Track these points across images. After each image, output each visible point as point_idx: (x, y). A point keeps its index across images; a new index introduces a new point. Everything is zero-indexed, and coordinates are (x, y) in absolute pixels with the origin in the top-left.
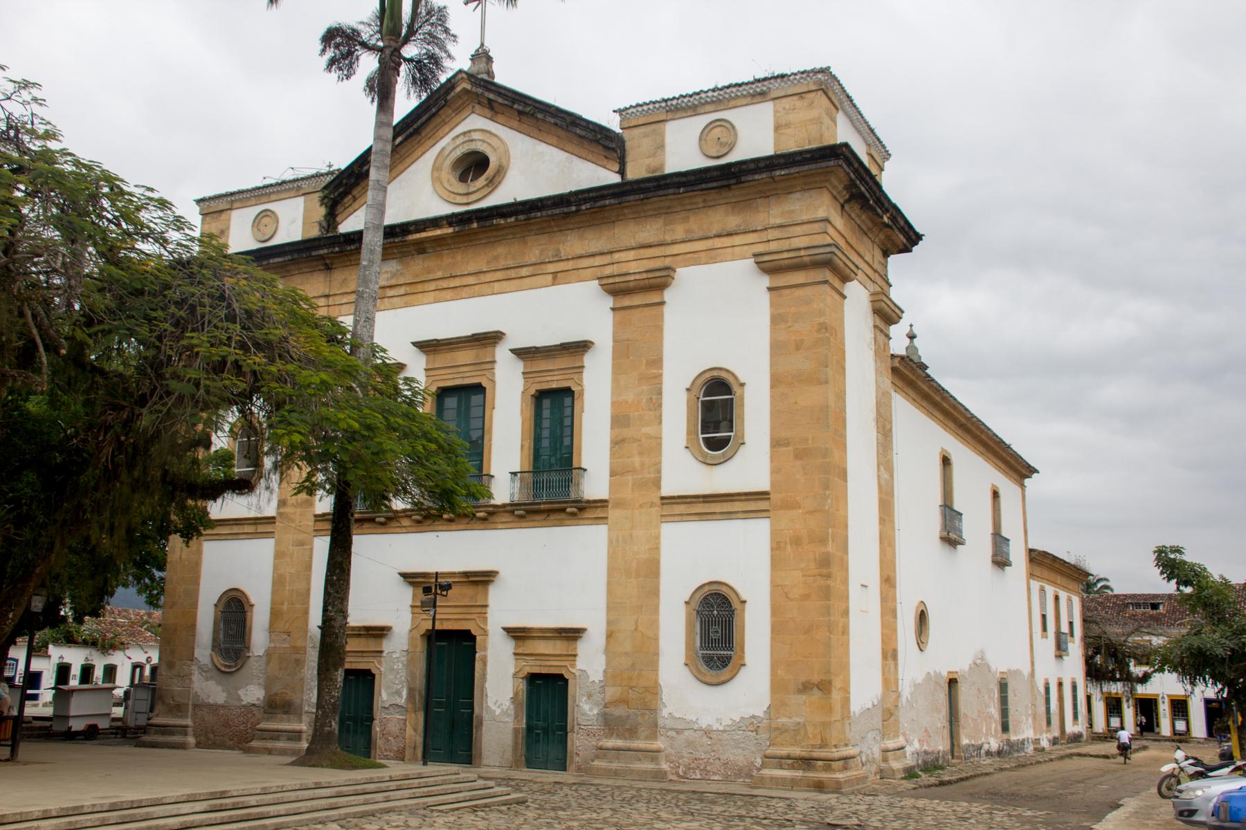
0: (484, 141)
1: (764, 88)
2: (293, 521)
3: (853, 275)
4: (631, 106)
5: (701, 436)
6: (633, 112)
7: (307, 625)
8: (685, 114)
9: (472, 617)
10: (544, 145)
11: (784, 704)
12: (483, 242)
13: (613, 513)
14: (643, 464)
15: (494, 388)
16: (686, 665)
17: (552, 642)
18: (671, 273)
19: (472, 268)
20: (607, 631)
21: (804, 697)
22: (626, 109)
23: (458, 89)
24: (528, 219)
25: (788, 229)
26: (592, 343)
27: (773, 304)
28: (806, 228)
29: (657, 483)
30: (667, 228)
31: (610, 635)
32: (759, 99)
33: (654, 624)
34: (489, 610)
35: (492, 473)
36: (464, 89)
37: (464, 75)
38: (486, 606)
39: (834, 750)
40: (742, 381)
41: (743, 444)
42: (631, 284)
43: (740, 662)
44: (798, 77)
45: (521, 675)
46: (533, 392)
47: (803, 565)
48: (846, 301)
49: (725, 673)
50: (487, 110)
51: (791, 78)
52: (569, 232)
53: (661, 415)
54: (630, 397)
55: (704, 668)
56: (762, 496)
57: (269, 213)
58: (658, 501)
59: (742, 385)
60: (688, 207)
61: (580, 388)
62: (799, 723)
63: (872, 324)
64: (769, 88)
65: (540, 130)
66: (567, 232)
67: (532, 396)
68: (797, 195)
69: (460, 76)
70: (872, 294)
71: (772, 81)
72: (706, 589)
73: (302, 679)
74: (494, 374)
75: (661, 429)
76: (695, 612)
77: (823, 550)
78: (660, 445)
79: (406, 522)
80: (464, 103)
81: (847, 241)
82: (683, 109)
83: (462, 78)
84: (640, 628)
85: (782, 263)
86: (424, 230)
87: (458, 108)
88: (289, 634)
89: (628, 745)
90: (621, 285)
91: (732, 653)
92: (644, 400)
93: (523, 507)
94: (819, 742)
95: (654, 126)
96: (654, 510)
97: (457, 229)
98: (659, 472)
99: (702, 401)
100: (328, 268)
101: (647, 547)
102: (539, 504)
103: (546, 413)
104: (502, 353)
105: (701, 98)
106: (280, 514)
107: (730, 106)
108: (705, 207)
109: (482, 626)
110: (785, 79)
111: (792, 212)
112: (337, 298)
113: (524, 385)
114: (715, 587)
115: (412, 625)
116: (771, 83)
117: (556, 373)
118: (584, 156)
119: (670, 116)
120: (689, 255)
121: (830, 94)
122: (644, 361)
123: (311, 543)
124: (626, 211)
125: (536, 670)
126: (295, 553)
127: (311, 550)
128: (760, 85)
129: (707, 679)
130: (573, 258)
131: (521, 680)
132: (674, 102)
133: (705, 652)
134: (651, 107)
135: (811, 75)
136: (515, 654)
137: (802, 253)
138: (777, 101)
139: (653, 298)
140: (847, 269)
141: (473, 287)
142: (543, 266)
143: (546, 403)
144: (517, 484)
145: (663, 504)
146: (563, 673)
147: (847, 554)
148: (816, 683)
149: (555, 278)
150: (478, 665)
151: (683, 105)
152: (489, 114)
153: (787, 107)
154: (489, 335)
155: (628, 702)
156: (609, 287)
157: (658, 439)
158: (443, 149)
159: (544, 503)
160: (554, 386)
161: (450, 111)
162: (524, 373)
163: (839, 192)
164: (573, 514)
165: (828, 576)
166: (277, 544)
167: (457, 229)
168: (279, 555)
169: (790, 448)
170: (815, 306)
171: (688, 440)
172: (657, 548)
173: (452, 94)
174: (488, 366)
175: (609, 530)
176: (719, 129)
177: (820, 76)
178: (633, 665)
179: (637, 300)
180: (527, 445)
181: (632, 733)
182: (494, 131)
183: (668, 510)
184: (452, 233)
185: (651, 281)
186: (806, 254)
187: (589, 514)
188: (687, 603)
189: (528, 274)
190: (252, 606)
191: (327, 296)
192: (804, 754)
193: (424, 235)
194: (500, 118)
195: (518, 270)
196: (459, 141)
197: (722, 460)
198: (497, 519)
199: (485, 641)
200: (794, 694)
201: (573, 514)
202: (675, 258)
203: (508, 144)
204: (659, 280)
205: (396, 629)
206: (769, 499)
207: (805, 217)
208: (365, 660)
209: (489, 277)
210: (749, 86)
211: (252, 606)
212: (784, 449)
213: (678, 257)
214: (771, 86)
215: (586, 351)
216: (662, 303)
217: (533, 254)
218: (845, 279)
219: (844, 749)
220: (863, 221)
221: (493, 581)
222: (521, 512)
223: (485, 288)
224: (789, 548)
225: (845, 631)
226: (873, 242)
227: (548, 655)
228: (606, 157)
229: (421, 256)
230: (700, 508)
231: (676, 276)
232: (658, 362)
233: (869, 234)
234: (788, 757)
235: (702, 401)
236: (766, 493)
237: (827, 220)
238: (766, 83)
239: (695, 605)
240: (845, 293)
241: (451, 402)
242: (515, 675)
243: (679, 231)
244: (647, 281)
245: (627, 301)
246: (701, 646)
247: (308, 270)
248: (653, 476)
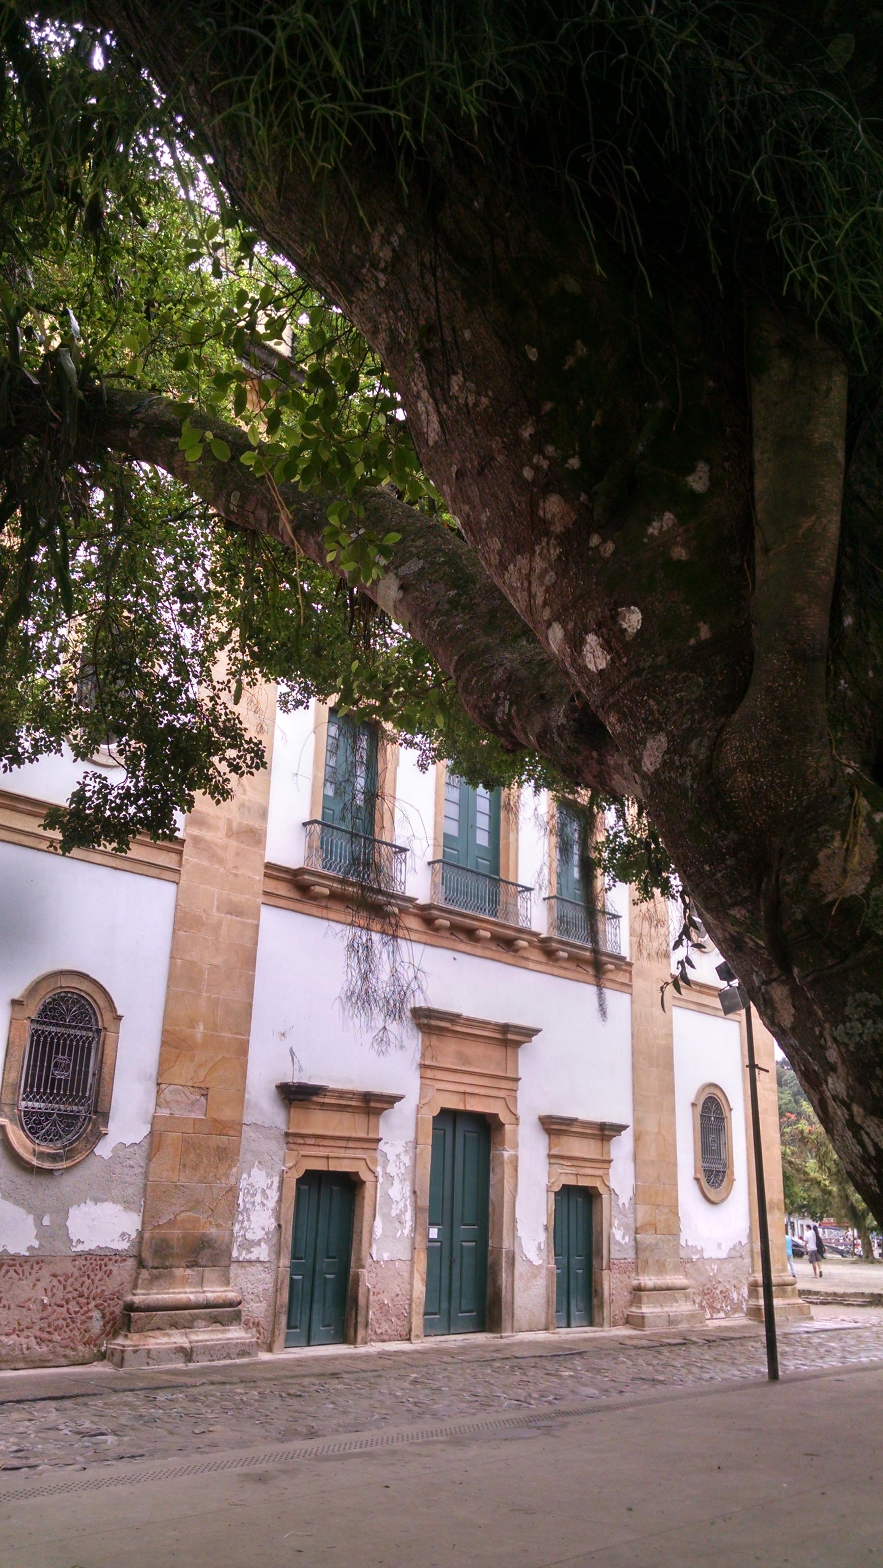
2: (221, 861)
7: (245, 1077)
38: (517, 1080)
73: (233, 1192)
88: (205, 1093)
93: (569, 949)
115: (421, 1097)
125: (572, 1181)
126: (224, 928)
127: (257, 926)
136: (550, 1156)
178: (659, 1177)
190: (119, 1018)
199: (515, 1133)
208: (350, 1153)
211: (119, 1018)
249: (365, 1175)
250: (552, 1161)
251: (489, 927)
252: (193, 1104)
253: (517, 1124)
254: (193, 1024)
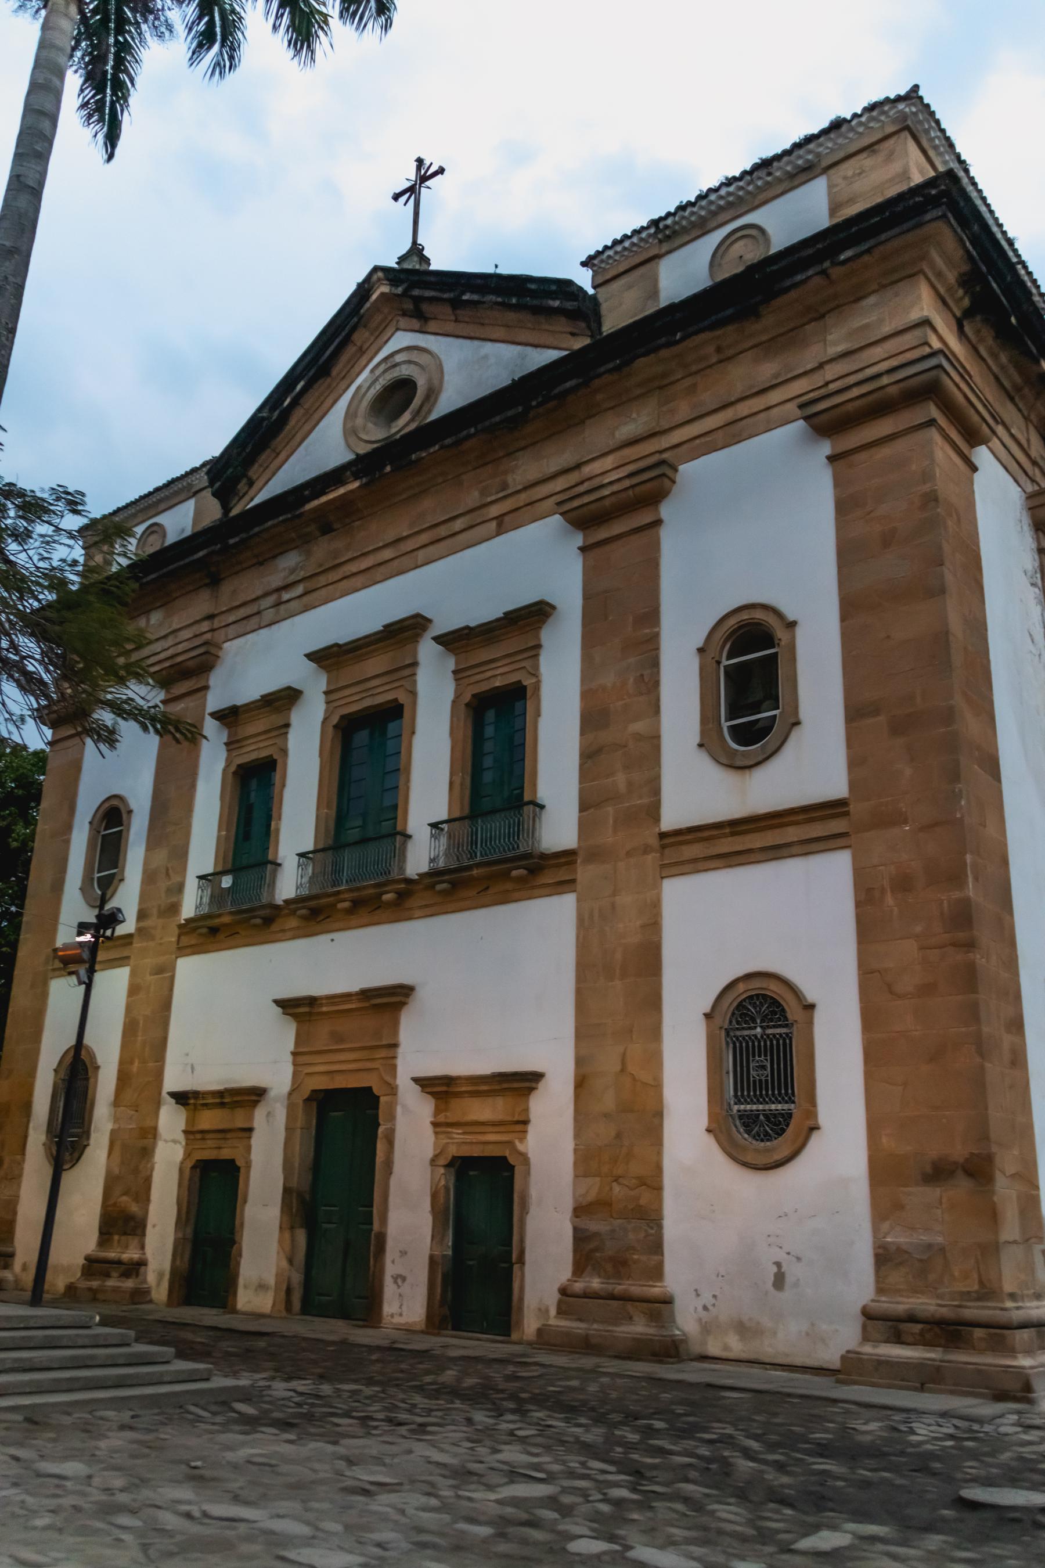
0: (409, 362)
1: (810, 157)
4: (606, 248)
5: (725, 725)
6: (609, 257)
8: (687, 238)
9: (375, 1065)
10: (489, 344)
11: (899, 1206)
12: (404, 496)
13: (584, 873)
14: (630, 784)
15: (414, 703)
16: (709, 1131)
17: (490, 1100)
18: (669, 472)
19: (390, 536)
20: (576, 1075)
21: (938, 1190)
22: (599, 253)
23: (374, 297)
24: (457, 443)
25: (857, 356)
26: (553, 607)
27: (838, 482)
28: (891, 346)
29: (654, 811)
30: (664, 409)
31: (581, 1083)
32: (803, 177)
33: (655, 1060)
34: (401, 1050)
35: (410, 831)
36: (382, 294)
37: (380, 274)
38: (395, 1046)
39: (1009, 1304)
40: (791, 617)
41: (798, 723)
42: (607, 503)
43: (810, 1123)
44: (863, 119)
45: (442, 1161)
46: (467, 697)
47: (918, 929)
48: (976, 476)
49: (781, 1146)
50: (415, 321)
51: (854, 123)
52: (520, 453)
53: (658, 700)
54: (608, 679)
55: (742, 1138)
56: (833, 808)
57: (155, 528)
58: (654, 842)
59: (792, 625)
60: (694, 368)
61: (534, 680)
62: (929, 1246)
63: (1034, 546)
64: (818, 155)
65: (483, 324)
66: (517, 454)
67: (467, 705)
68: (872, 300)
69: (375, 277)
70: (1030, 497)
71: (822, 139)
72: (741, 987)
74: (415, 682)
75: (659, 722)
76: (723, 1033)
77: (956, 895)
78: (657, 749)
79: (293, 923)
80: (386, 318)
82: (685, 230)
83: (379, 280)
84: (631, 1068)
85: (850, 407)
86: (323, 493)
87: (377, 327)
89: (610, 1287)
90: (593, 506)
91: (793, 1105)
92: (631, 680)
93: (446, 877)
94: (976, 1287)
95: (642, 270)
96: (649, 857)
97: (364, 480)
98: (656, 792)
99: (725, 667)
100: (214, 581)
101: (638, 923)
102: (469, 868)
103: (489, 731)
104: (427, 650)
105: (711, 203)
106: (139, 930)
107: (757, 203)
108: (720, 361)
109: (388, 1079)
110: (844, 128)
111: (866, 327)
112: (222, 617)
113: (456, 691)
114: (756, 984)
116: (821, 145)
117: (499, 664)
118: (542, 342)
119: (665, 247)
120: (698, 441)
121: (925, 144)
122: (631, 619)
123: (173, 969)
124: (599, 397)
125: (466, 1151)
127: (172, 979)
128: (801, 152)
129: (749, 1158)
130: (525, 489)
131: (442, 1170)
132: (669, 221)
133: (742, 1107)
134: (635, 240)
135: (886, 108)
136: (435, 1124)
137: (885, 380)
138: (832, 172)
139: (644, 518)
140: (972, 412)
141: (391, 563)
142: (484, 511)
143: (490, 715)
144: (444, 840)
145: (663, 847)
146: (507, 1154)
148: (961, 1160)
149: (500, 525)
150: (381, 1147)
151: (684, 223)
152: (416, 324)
153: (850, 173)
154: (406, 623)
155: (610, 1205)
156: (575, 514)
157: (654, 740)
158: (359, 388)
159: (478, 865)
160: (498, 684)
161: (367, 334)
162: (455, 672)
163: (949, 289)
164: (520, 880)
165: (970, 945)
166: (133, 974)
167: (364, 480)
168: (133, 990)
169: (882, 718)
170: (914, 467)
171: (703, 733)
172: (653, 925)
173: (368, 305)
174: (407, 672)
175: (578, 900)
176: (741, 243)
177: (901, 106)
178: (618, 1136)
179: (618, 528)
180: (458, 780)
181: (620, 1266)
182: (422, 344)
183: (671, 855)
184: (359, 487)
185: (638, 489)
186: (893, 380)
187: (548, 877)
188: (707, 1016)
189: (463, 527)
191: (211, 617)
192: (944, 1312)
193: (324, 499)
194: (432, 326)
195: (450, 524)
196: (378, 372)
197: (760, 758)
198: (414, 902)
201: (520, 880)
202: (676, 451)
203: (443, 357)
204: (649, 485)
205: (272, 1094)
206: (847, 814)
207: (887, 329)
209: (410, 545)
210: (785, 159)
212: (870, 721)
213: (685, 447)
214: (820, 149)
215: (544, 622)
216: (658, 523)
217: (472, 498)
219: (1035, 1303)
220: (1002, 368)
221: (403, 1004)
222: (444, 886)
223: (406, 561)
224: (889, 900)
225: (1018, 1059)
226: (1026, 419)
227: (483, 1124)
228: (573, 334)
229: (326, 537)
230: (726, 845)
231: (678, 478)
232: (651, 616)
233: (1017, 399)
234: (911, 1318)
235: (725, 667)
236: (841, 803)
237: (926, 322)
238: (811, 146)
239: (723, 1020)
241: (362, 737)
242: (433, 1161)
243: (684, 409)
244: (630, 492)
245: (603, 534)
246: (736, 1096)
247: (191, 588)
248: (645, 801)
250: (438, 1130)
251: (346, 896)
252: (131, 1118)
253: (395, 1094)
254: (132, 1063)
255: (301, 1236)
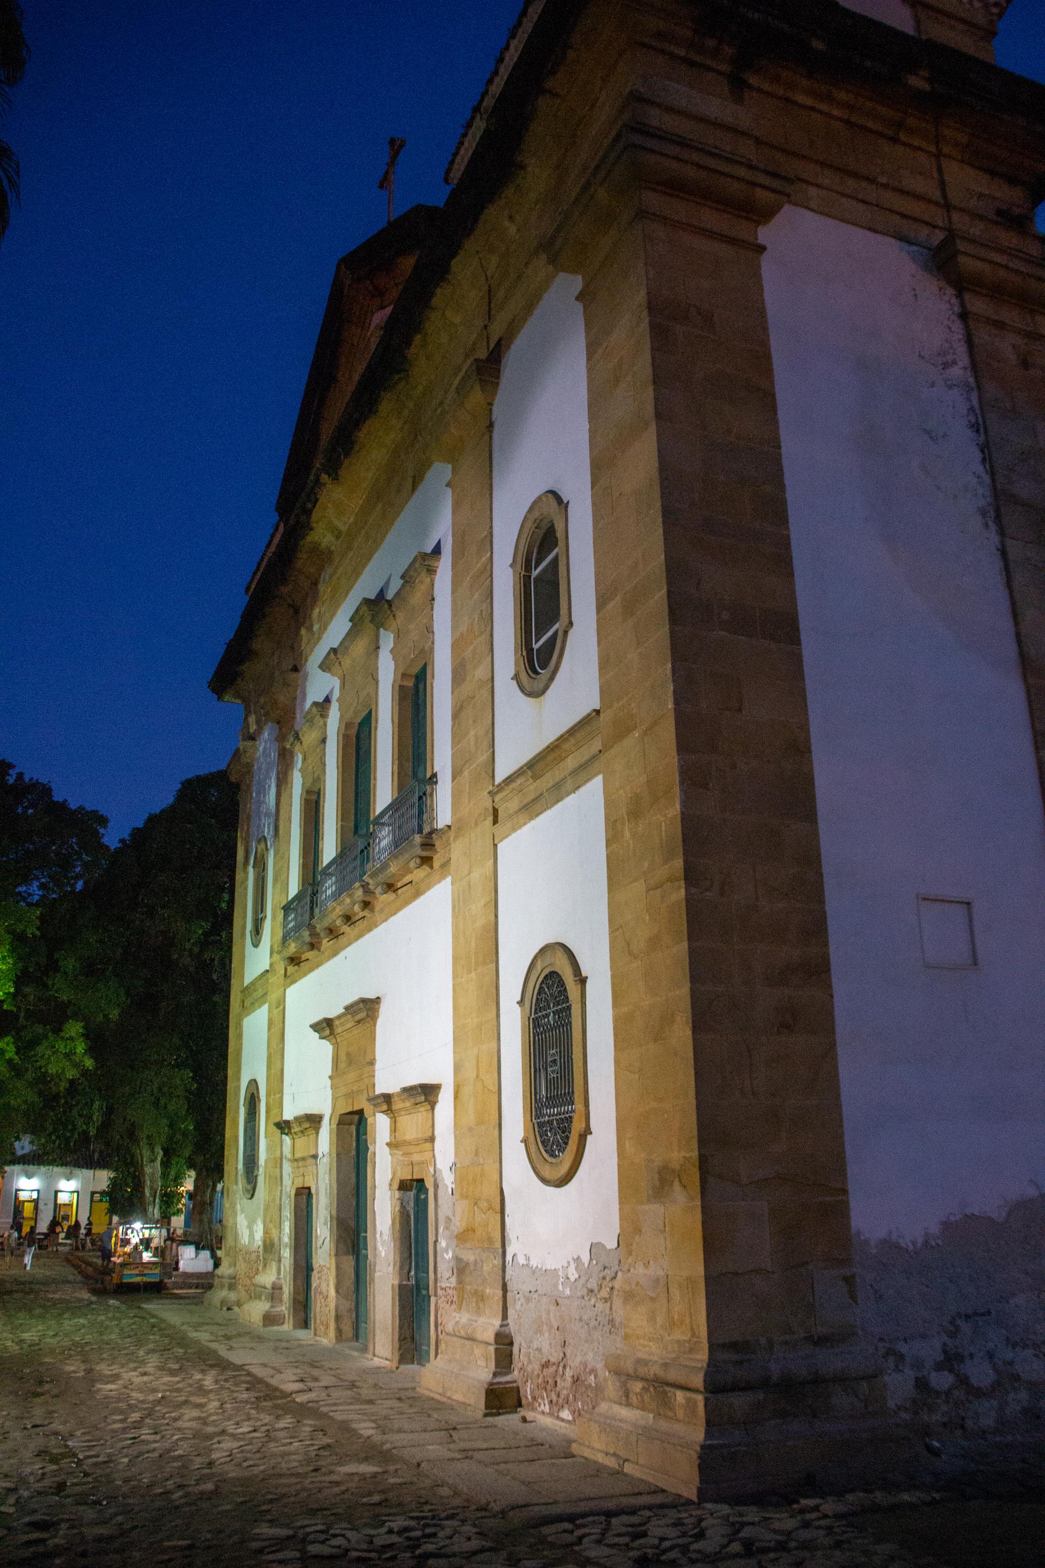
3: (761, 194)
34: (378, 1066)
49: (566, 1158)
72: (539, 966)
81: (758, 141)
127: (284, 1008)
147: (810, 816)
200: (649, 1201)
218: (765, 215)
233: (903, 137)
240: (761, 240)
249: (313, 1191)
255: (349, 1262)
